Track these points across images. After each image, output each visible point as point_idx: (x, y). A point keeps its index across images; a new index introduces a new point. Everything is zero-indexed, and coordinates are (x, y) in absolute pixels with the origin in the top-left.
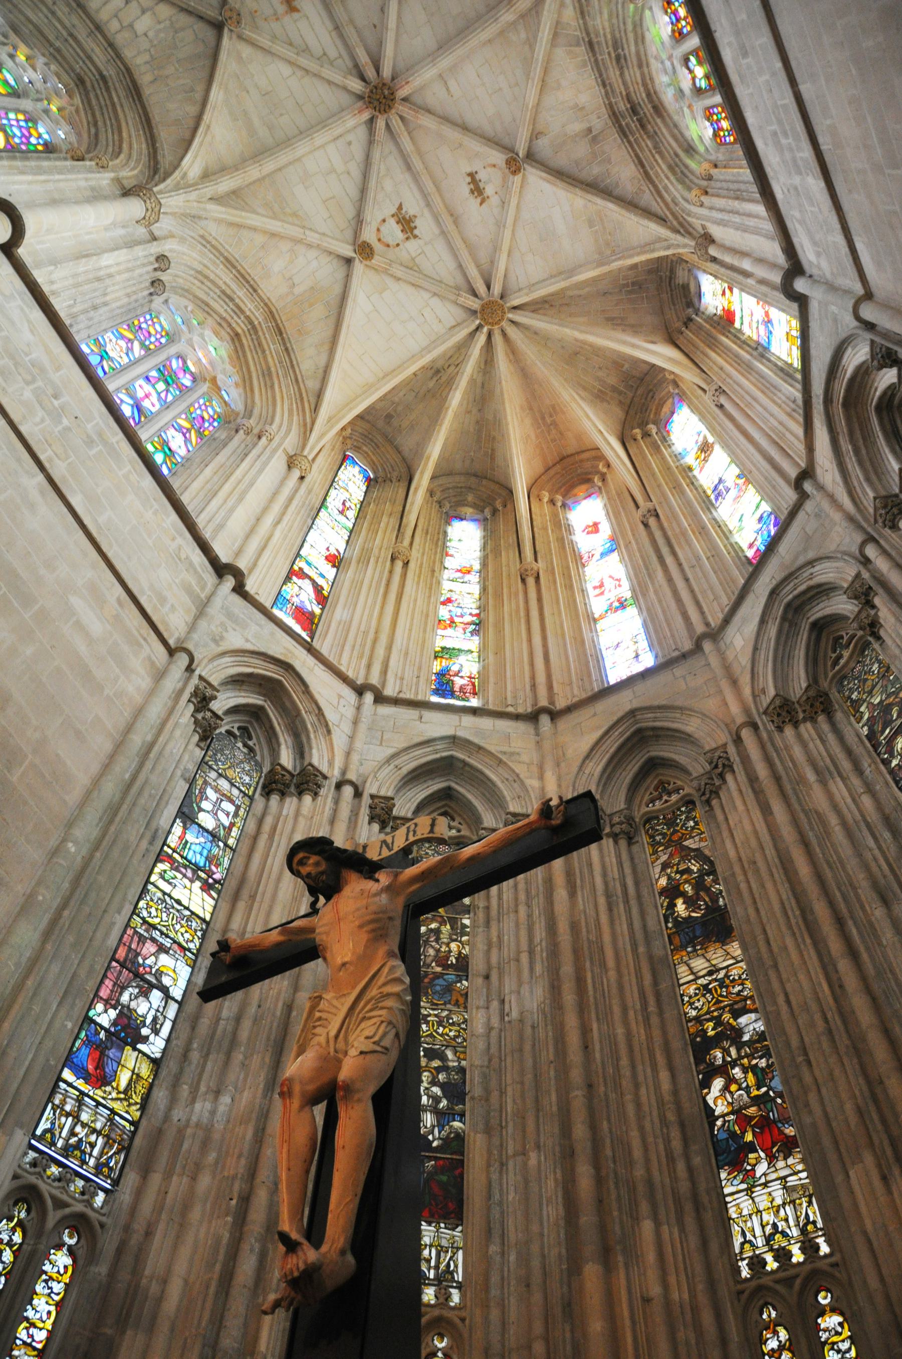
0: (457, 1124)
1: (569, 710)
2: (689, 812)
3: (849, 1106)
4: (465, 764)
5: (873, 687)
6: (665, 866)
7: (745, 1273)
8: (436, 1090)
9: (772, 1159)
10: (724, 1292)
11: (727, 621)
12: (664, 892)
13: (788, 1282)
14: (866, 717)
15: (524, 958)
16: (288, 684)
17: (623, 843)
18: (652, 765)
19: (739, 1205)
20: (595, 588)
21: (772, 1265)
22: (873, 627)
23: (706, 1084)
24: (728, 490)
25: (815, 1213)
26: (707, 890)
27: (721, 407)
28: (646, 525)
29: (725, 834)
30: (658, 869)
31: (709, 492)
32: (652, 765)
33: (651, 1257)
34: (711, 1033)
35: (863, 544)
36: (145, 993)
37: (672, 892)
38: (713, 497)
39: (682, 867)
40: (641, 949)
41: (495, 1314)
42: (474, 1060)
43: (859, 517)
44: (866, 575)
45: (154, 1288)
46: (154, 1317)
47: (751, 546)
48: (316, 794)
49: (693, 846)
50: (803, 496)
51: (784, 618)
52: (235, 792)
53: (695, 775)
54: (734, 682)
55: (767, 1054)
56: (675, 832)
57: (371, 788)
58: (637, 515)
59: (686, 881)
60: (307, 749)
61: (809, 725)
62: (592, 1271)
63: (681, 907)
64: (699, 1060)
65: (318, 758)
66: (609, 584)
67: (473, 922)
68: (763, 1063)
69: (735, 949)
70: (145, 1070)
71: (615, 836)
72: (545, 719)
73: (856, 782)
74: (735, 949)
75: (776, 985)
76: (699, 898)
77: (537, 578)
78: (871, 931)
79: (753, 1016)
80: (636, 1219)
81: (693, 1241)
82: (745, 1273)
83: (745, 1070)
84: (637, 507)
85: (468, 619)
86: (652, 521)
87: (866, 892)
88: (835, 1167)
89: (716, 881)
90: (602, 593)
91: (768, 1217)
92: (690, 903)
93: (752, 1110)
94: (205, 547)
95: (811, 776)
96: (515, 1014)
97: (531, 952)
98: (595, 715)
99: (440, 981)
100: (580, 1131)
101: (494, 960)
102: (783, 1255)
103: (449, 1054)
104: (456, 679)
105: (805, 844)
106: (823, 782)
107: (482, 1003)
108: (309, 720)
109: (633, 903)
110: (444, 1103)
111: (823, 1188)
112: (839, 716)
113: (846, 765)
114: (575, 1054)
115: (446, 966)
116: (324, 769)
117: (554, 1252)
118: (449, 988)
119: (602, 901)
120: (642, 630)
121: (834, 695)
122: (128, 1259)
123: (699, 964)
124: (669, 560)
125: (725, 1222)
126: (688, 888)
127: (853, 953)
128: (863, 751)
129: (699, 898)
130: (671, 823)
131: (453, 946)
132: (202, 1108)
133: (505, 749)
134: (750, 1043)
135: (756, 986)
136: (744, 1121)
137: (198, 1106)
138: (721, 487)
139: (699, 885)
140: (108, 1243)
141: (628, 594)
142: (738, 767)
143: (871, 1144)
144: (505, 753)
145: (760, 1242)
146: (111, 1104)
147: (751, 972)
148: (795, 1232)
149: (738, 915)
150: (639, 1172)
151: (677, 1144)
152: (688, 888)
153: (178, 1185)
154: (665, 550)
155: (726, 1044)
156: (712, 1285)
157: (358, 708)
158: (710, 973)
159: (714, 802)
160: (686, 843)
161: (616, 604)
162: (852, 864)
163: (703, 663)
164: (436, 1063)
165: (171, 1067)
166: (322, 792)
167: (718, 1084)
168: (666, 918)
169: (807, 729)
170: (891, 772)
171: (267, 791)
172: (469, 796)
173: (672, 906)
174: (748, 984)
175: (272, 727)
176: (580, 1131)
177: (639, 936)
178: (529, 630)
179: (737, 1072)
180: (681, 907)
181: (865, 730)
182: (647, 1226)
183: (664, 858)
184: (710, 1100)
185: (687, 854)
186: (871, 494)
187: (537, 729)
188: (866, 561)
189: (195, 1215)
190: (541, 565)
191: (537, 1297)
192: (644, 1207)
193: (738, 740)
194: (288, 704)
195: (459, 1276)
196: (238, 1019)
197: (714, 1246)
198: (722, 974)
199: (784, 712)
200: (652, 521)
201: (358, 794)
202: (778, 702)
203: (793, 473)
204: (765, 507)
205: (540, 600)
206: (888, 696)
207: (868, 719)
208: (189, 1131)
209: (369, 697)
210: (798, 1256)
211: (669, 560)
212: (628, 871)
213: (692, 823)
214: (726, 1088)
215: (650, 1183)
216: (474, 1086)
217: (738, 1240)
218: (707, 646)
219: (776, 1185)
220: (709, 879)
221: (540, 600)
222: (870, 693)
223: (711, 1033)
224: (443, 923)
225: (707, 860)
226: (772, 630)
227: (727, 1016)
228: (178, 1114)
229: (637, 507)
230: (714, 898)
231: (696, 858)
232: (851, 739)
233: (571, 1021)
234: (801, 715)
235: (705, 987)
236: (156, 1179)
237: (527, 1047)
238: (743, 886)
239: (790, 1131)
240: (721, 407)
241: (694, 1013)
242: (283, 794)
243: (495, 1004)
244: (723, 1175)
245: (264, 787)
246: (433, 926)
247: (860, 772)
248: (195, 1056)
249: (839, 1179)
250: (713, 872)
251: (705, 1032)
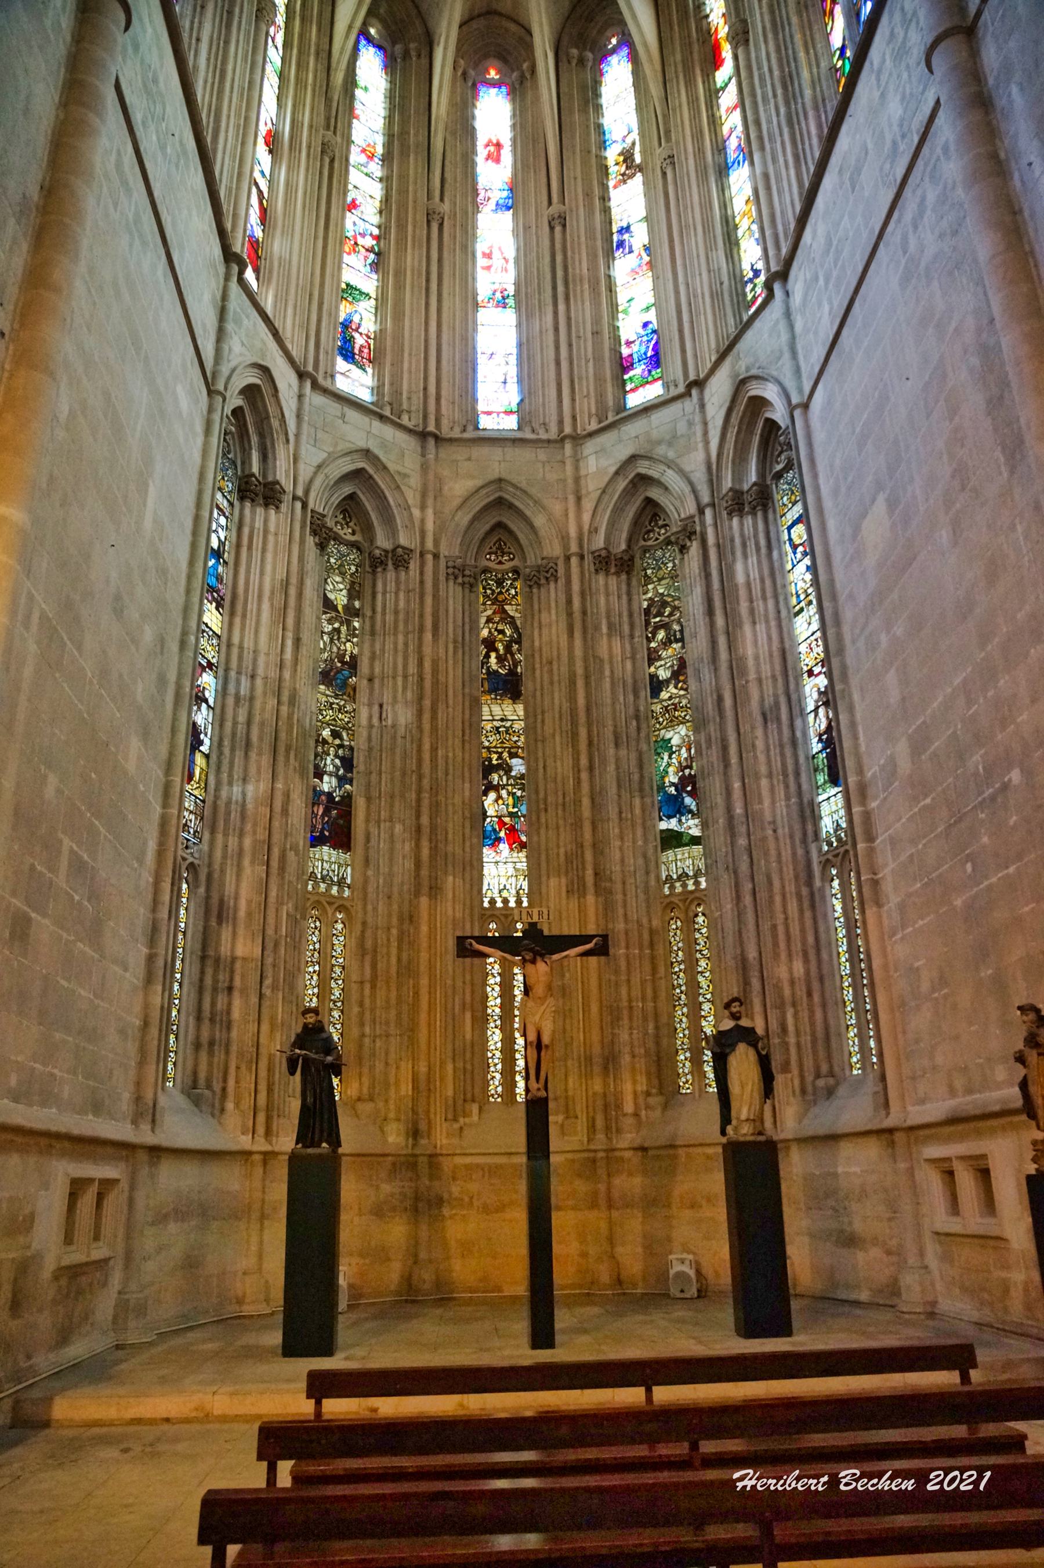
0: (348, 787)
1: (451, 440)
2: (514, 580)
3: (562, 851)
4: (371, 477)
5: (663, 578)
6: (489, 620)
7: (486, 905)
8: (337, 761)
9: (512, 849)
10: (476, 910)
11: (591, 435)
12: (485, 641)
13: (506, 916)
14: (650, 595)
15: (400, 681)
16: (266, 390)
17: (467, 591)
18: (500, 525)
19: (489, 870)
20: (484, 255)
21: (499, 905)
22: (683, 549)
23: (485, 793)
24: (631, 252)
25: (525, 885)
26: (512, 655)
27: (664, 174)
28: (552, 228)
29: (536, 624)
30: (483, 620)
31: (615, 230)
32: (500, 525)
33: (450, 895)
34: (495, 762)
35: (708, 505)
36: (199, 709)
37: (490, 644)
38: (615, 238)
39: (500, 627)
40: (467, 690)
41: (370, 907)
42: (360, 743)
43: (714, 467)
44: (697, 519)
45: (232, 903)
46: (235, 919)
47: (629, 343)
48: (277, 508)
49: (511, 613)
50: (688, 394)
51: (632, 481)
52: (225, 503)
53: (528, 563)
54: (579, 499)
55: (523, 789)
56: (501, 593)
57: (311, 505)
58: (546, 213)
59: (501, 641)
60: (270, 455)
61: (615, 578)
62: (424, 901)
63: (493, 659)
64: (485, 777)
65: (282, 472)
66: (497, 262)
67: (362, 628)
68: (519, 793)
69: (520, 709)
70: (204, 761)
71: (463, 584)
72: (431, 442)
73: (628, 646)
74: (520, 709)
75: (540, 754)
76: (506, 659)
77: (441, 225)
78: (604, 762)
79: (520, 761)
80: (446, 873)
81: (468, 886)
82: (486, 905)
83: (509, 794)
84: (550, 203)
85: (369, 242)
86: (558, 229)
87: (608, 732)
88: (544, 872)
89: (519, 651)
90: (488, 268)
91: (503, 881)
92: (500, 659)
93: (507, 820)
94: (222, 233)
95: (605, 630)
96: (390, 722)
97: (405, 677)
98: (469, 459)
99: (340, 676)
100: (425, 820)
101: (377, 670)
102: (505, 901)
103: (344, 734)
104: (356, 335)
105: (587, 677)
106: (610, 636)
107: (366, 701)
108: (275, 423)
109: (467, 648)
110: (341, 772)
111: (534, 874)
112: (634, 582)
113: (626, 628)
114: (426, 769)
115: (343, 663)
116: (283, 482)
117: (406, 887)
118: (345, 684)
119: (451, 646)
120: (515, 351)
121: (637, 560)
122: (215, 885)
123: (497, 710)
124: (561, 307)
125: (481, 876)
126: (500, 647)
127: (591, 768)
128: (639, 620)
129: (506, 659)
130: (500, 583)
131: (348, 644)
132: (236, 790)
133: (400, 468)
134: (515, 778)
135: (526, 742)
136: (502, 824)
137: (235, 789)
138: (626, 236)
139: (508, 648)
140: (203, 877)
141: (511, 290)
142: (562, 581)
143: (567, 872)
144: (399, 473)
145: (496, 891)
146: (196, 792)
147: (526, 730)
148: (514, 892)
149: (527, 687)
150: (450, 848)
151: (467, 831)
152: (500, 647)
153: (233, 842)
154: (560, 289)
155: (502, 773)
156: (472, 909)
157: (300, 397)
158: (502, 720)
159: (535, 590)
160: (507, 607)
161: (498, 295)
162: (609, 709)
163: (559, 457)
164: (337, 742)
165: (214, 758)
166: (284, 507)
167: (492, 796)
168: (483, 664)
169: (613, 581)
170: (649, 649)
171: (242, 499)
172: (369, 508)
173: (487, 656)
174: (522, 738)
175: (245, 424)
176: (425, 820)
177: (467, 678)
178: (427, 304)
179: (504, 793)
180: (493, 659)
181: (645, 604)
182: (450, 878)
183: (489, 612)
184: (486, 804)
185: (507, 618)
186: (730, 485)
187: (423, 447)
188: (701, 511)
189: (246, 862)
190: (446, 207)
191: (395, 907)
192: (450, 868)
193: (568, 558)
194: (260, 404)
195: (349, 881)
196: (249, 723)
197: (475, 892)
198: (508, 724)
199: (604, 562)
200: (558, 229)
201: (305, 506)
202: (604, 553)
203: (692, 377)
204: (652, 316)
205: (440, 260)
206: (669, 595)
207: (650, 599)
208: (233, 806)
209: (308, 384)
210: (512, 904)
211: (561, 307)
212: (467, 620)
213: (513, 592)
214: (496, 801)
215: (454, 855)
216: (359, 760)
217: (485, 887)
218: (568, 446)
219: (511, 865)
220: (515, 647)
221: (440, 260)
222: (660, 580)
223: (495, 762)
224: (342, 624)
225: (516, 628)
226: (622, 484)
227: (505, 755)
228: (224, 793)
229: (550, 203)
230: (516, 663)
231: (510, 623)
232: (635, 607)
233: (427, 746)
234: (613, 570)
235: (497, 728)
236: (220, 837)
237: (398, 751)
238: (538, 672)
239: (524, 838)
240: (664, 174)
241: (487, 744)
242: (253, 501)
243: (376, 708)
244: (485, 850)
245: (239, 491)
246: (336, 625)
247: (632, 636)
248: (227, 751)
249: (544, 879)
250: (518, 642)
251: (490, 760)
